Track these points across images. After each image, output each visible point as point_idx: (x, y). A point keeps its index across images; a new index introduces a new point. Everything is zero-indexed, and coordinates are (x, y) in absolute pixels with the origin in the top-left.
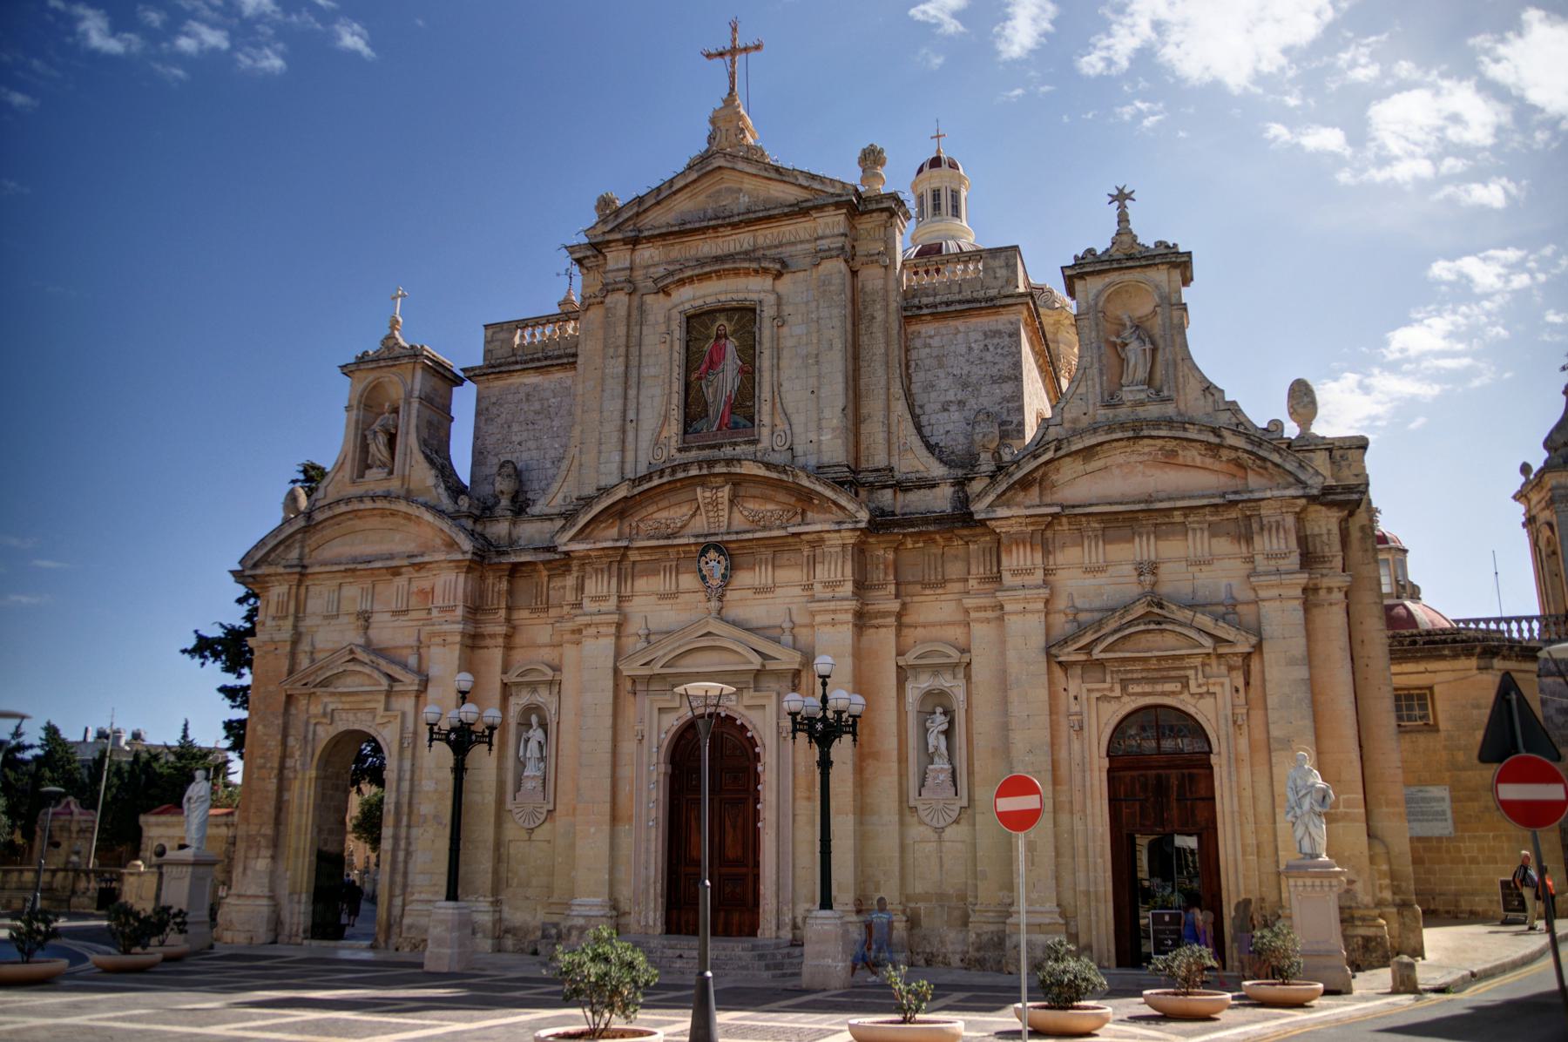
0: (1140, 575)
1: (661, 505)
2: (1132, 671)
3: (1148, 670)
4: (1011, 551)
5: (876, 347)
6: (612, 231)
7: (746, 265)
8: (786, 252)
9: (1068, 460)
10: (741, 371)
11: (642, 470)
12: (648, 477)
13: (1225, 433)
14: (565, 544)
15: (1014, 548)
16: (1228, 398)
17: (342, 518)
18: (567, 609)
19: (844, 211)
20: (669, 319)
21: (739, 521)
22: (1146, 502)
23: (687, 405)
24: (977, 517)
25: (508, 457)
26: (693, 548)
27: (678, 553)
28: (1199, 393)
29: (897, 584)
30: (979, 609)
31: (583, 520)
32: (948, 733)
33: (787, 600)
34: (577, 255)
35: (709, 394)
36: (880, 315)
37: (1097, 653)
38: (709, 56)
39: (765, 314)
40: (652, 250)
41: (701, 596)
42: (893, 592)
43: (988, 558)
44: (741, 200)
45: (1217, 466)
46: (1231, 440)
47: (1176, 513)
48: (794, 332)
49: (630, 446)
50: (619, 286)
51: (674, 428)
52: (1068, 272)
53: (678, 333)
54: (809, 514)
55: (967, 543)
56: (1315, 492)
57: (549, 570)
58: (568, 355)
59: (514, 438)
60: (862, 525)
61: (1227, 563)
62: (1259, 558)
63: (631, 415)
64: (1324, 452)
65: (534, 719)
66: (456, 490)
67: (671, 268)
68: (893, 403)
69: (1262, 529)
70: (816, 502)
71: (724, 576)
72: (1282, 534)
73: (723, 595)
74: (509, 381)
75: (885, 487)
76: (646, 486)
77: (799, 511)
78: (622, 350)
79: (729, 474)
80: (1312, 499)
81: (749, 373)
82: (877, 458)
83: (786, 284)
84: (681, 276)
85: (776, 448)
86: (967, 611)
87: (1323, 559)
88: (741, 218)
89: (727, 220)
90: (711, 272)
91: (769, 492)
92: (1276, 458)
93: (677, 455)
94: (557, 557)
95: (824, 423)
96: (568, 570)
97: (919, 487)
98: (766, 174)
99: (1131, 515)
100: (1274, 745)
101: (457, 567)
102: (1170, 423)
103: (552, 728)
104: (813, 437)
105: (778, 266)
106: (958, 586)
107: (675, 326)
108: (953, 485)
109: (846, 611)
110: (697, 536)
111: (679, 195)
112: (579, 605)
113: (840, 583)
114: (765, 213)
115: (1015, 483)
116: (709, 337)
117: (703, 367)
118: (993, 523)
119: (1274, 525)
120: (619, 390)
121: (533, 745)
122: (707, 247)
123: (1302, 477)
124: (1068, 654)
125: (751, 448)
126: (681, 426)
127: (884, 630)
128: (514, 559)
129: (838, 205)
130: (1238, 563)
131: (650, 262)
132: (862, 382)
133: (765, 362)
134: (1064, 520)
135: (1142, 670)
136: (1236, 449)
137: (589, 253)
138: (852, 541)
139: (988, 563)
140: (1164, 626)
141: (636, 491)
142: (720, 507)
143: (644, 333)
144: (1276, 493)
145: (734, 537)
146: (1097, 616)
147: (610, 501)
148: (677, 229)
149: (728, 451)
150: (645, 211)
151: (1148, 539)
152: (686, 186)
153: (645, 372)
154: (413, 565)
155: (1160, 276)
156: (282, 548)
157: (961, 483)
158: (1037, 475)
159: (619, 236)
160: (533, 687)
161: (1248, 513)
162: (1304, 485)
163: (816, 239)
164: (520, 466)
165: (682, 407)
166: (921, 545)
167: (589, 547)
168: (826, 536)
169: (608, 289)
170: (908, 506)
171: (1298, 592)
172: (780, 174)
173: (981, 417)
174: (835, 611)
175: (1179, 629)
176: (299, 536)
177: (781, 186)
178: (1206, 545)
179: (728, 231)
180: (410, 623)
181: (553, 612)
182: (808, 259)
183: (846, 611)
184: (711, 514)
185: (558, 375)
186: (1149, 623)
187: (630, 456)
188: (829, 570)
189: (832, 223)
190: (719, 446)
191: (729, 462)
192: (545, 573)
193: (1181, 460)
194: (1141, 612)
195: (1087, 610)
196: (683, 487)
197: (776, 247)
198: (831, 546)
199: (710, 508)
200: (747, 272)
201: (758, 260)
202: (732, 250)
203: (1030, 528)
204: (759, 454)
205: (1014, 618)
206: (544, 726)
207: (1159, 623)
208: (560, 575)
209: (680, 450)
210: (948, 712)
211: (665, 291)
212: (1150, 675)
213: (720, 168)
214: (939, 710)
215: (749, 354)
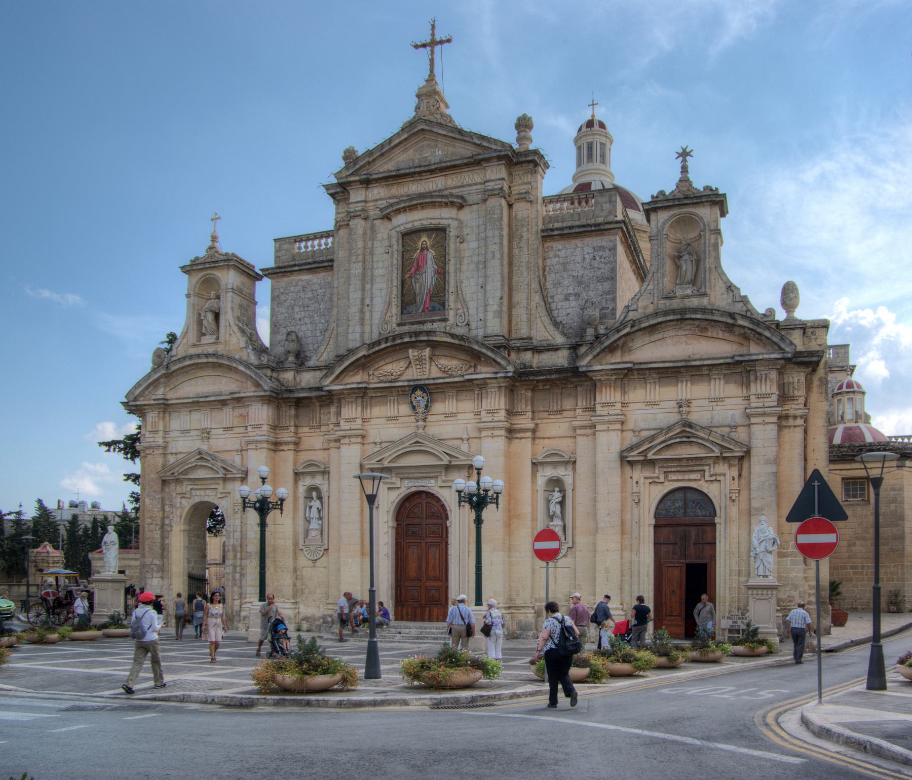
0: (680, 407)
1: (387, 361)
2: (671, 467)
3: (681, 466)
4: (602, 392)
5: (524, 256)
6: (352, 174)
7: (439, 200)
8: (464, 191)
9: (639, 333)
11: (375, 337)
12: (378, 343)
13: (737, 317)
14: (327, 386)
15: (604, 389)
16: (742, 294)
18: (331, 426)
20: (390, 237)
21: (435, 372)
22: (686, 361)
23: (403, 295)
24: (581, 370)
25: (293, 329)
26: (407, 388)
27: (398, 392)
28: (724, 289)
29: (533, 412)
30: (582, 427)
31: (338, 370)
32: (562, 503)
33: (465, 421)
34: (332, 191)
36: (525, 234)
38: (416, 47)
39: (452, 234)
41: (413, 419)
42: (530, 416)
43: (588, 396)
44: (437, 154)
45: (732, 338)
46: (741, 322)
47: (704, 368)
48: (472, 245)
49: (367, 322)
50: (358, 213)
51: (395, 310)
53: (396, 247)
54: (479, 367)
55: (576, 386)
56: (789, 356)
57: (320, 402)
59: (296, 316)
60: (510, 374)
61: (734, 401)
62: (753, 398)
63: (368, 301)
64: (799, 330)
65: (314, 494)
66: (261, 350)
67: (391, 201)
68: (533, 295)
70: (483, 359)
71: (426, 406)
72: (768, 383)
73: (426, 418)
74: (291, 278)
75: (526, 350)
76: (377, 348)
77: (473, 364)
78: (360, 258)
79: (429, 341)
80: (788, 360)
81: (442, 273)
82: (522, 331)
83: (466, 215)
85: (459, 324)
86: (575, 429)
87: (793, 399)
88: (436, 166)
89: (427, 168)
91: (454, 353)
92: (767, 334)
93: (397, 328)
94: (323, 393)
95: (489, 308)
96: (332, 403)
97: (548, 350)
99: (676, 370)
101: (262, 400)
102: (704, 310)
103: (325, 499)
104: (481, 316)
106: (571, 413)
107: (394, 241)
108: (569, 349)
109: (501, 428)
110: (409, 381)
111: (396, 150)
112: (338, 424)
113: (496, 411)
115: (605, 348)
116: (416, 250)
117: (413, 269)
118: (591, 374)
119: (764, 376)
120: (359, 283)
121: (314, 510)
122: (414, 188)
123: (783, 346)
124: (634, 456)
125: (443, 324)
126: (399, 309)
127: (524, 440)
128: (297, 395)
130: (739, 401)
131: (378, 197)
132: (514, 280)
133: (451, 268)
134: (635, 372)
135: (677, 466)
136: (744, 327)
137: (338, 190)
139: (588, 399)
140: (692, 439)
141: (371, 352)
142: (424, 362)
143: (375, 246)
144: (766, 356)
145: (432, 382)
146: (653, 433)
149: (428, 327)
150: (374, 160)
151: (687, 385)
153: (376, 272)
154: (234, 399)
156: (152, 387)
157: (574, 348)
158: (620, 343)
159: (357, 178)
160: (313, 474)
161: (748, 369)
162: (783, 351)
163: (485, 182)
164: (300, 334)
165: (399, 296)
166: (548, 387)
167: (342, 387)
168: (489, 381)
169: (352, 216)
170: (541, 362)
171: (775, 419)
173: (588, 305)
174: (493, 428)
175: (700, 441)
176: (162, 380)
177: (462, 145)
178: (722, 389)
180: (235, 436)
181: (323, 428)
182: (480, 196)
183: (501, 428)
184: (418, 367)
185: (322, 275)
186: (683, 437)
187: (367, 329)
188: (491, 403)
190: (422, 323)
191: (428, 333)
193: (709, 334)
194: (679, 430)
195: (646, 429)
196: (400, 349)
197: (459, 187)
199: (418, 363)
201: (446, 196)
202: (431, 189)
204: (448, 328)
205: (601, 434)
206: (320, 498)
207: (689, 437)
209: (399, 325)
210: (563, 491)
211: (388, 217)
212: (682, 469)
213: (423, 130)
214: (557, 489)
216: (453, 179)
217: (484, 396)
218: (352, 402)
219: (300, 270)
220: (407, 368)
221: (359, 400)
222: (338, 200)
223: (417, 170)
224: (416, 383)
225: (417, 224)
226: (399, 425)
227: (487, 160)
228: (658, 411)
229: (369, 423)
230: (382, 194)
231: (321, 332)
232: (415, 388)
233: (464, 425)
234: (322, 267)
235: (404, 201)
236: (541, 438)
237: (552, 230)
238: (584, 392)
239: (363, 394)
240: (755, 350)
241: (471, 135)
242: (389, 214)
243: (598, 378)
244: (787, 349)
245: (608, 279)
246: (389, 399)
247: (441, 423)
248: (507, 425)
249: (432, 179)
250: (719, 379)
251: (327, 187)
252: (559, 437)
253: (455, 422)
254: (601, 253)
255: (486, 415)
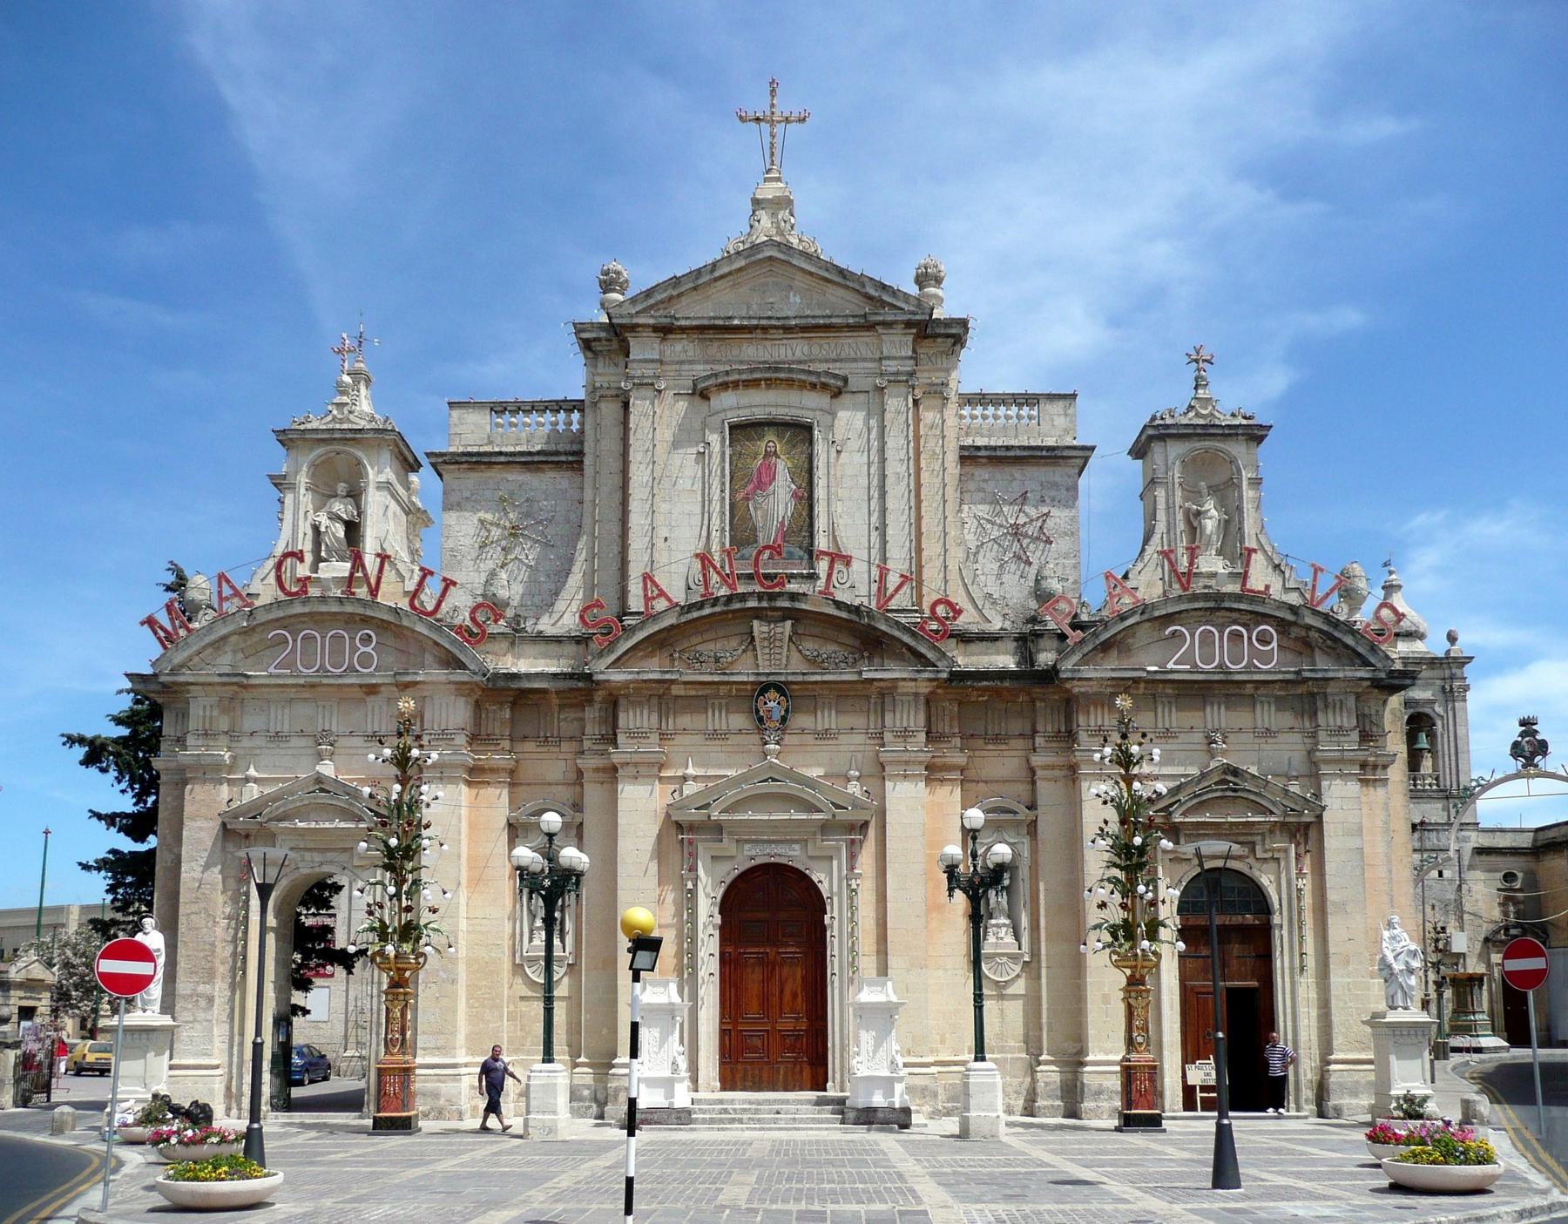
1: (706, 637)
7: (803, 377)
9: (1147, 625)
10: (795, 495)
14: (602, 673)
15: (1092, 709)
17: (293, 620)
19: (914, 331)
27: (731, 690)
30: (1047, 767)
33: (852, 748)
35: (758, 517)
37: (1177, 818)
40: (685, 342)
46: (1309, 620)
47: (1248, 685)
52: (1151, 432)
55: (1033, 701)
58: (574, 453)
62: (1322, 735)
63: (663, 532)
69: (1326, 707)
71: (784, 719)
72: (1345, 714)
73: (782, 739)
76: (695, 614)
81: (806, 500)
84: (726, 379)
85: (837, 585)
90: (760, 380)
96: (590, 702)
98: (826, 275)
100: (1330, 908)
105: (840, 383)
108: (1016, 640)
109: (920, 763)
112: (614, 743)
114: (827, 321)
116: (757, 454)
117: (751, 487)
129: (909, 324)
130: (1297, 737)
131: (683, 357)
133: (820, 492)
136: (1309, 628)
137: (603, 335)
138: (926, 691)
140: (1239, 794)
141: (683, 619)
145: (800, 678)
147: (656, 628)
148: (721, 322)
151: (1219, 709)
152: (730, 273)
155: (1237, 449)
168: (901, 684)
172: (844, 277)
174: (907, 763)
177: (841, 292)
179: (779, 334)
184: (767, 651)
188: (902, 719)
189: (898, 345)
192: (555, 701)
198: (904, 694)
199: (766, 644)
200: (802, 386)
202: (783, 357)
203: (1109, 690)
208: (572, 706)
211: (704, 395)
213: (771, 258)
215: (806, 476)
216: (821, 346)
217: (888, 706)
218: (640, 704)
219: (508, 463)
220: (744, 651)
221: (655, 701)
222: (595, 353)
223: (763, 322)
224: (771, 678)
225: (760, 414)
226: (730, 749)
227: (888, 325)
228: (1174, 747)
229: (671, 742)
230: (691, 353)
231: (548, 576)
232: (764, 688)
233: (849, 755)
234: (552, 462)
235: (761, 370)
236: (973, 781)
237: (978, 448)
238: (1049, 711)
239: (661, 696)
240: (1324, 665)
241: (861, 279)
242: (707, 389)
243: (1083, 690)
244: (1379, 665)
245: (1066, 534)
246: (710, 701)
247: (809, 748)
248: (927, 757)
249: (785, 341)
250: (1269, 703)
251: (579, 328)
252: (1004, 781)
253: (834, 748)
254: (1053, 493)
255: (892, 739)
